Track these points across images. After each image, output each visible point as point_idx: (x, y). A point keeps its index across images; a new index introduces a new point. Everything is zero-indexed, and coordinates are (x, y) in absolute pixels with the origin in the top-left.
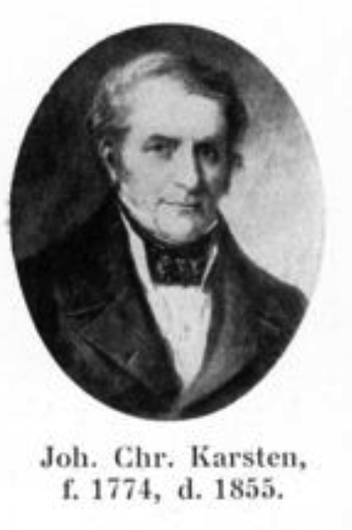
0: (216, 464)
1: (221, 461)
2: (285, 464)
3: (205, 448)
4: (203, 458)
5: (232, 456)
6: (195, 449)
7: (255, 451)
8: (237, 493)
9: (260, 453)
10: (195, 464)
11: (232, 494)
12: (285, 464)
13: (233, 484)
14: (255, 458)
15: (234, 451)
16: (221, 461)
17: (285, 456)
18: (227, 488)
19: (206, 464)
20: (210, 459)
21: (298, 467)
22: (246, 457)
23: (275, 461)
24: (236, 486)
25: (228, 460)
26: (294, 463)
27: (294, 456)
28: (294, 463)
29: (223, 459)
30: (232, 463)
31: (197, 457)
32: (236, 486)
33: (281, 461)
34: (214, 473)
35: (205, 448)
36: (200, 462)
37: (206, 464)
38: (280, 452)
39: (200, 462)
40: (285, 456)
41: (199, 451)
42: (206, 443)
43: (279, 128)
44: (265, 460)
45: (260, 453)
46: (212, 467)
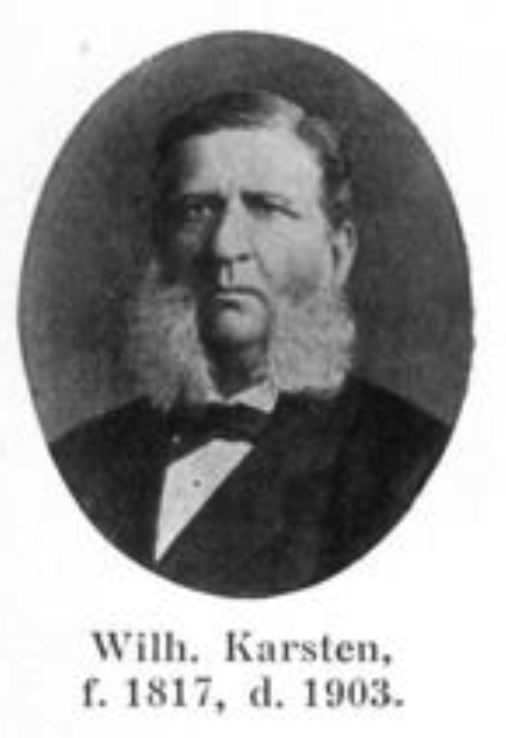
0: (261, 658)
1: (269, 653)
2: (362, 658)
3: (246, 635)
4: (242, 648)
5: (286, 647)
6: (231, 636)
7: (318, 640)
8: (156, 698)
9: (325, 642)
10: (231, 657)
11: (150, 699)
12: (362, 658)
13: (151, 685)
14: (319, 650)
15: (290, 638)
16: (269, 653)
17: (362, 646)
18: (143, 691)
19: (247, 657)
20: (253, 651)
21: (380, 663)
22: (305, 648)
23: (346, 654)
24: (157, 689)
25: (279, 652)
26: (374, 658)
27: (374, 647)
28: (374, 658)
29: (272, 649)
30: (286, 657)
31: (234, 648)
32: (157, 689)
33: (356, 653)
34: (129, 666)
35: (246, 635)
36: (238, 654)
37: (247, 657)
38: (355, 639)
39: (238, 654)
40: (362, 646)
41: (237, 640)
42: (249, 627)
43: (189, 374)
44: (332, 653)
45: (325, 642)
46: (255, 663)
